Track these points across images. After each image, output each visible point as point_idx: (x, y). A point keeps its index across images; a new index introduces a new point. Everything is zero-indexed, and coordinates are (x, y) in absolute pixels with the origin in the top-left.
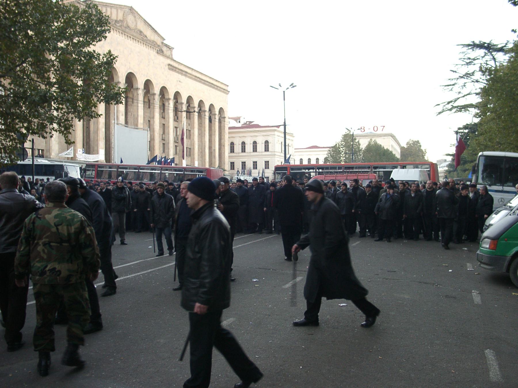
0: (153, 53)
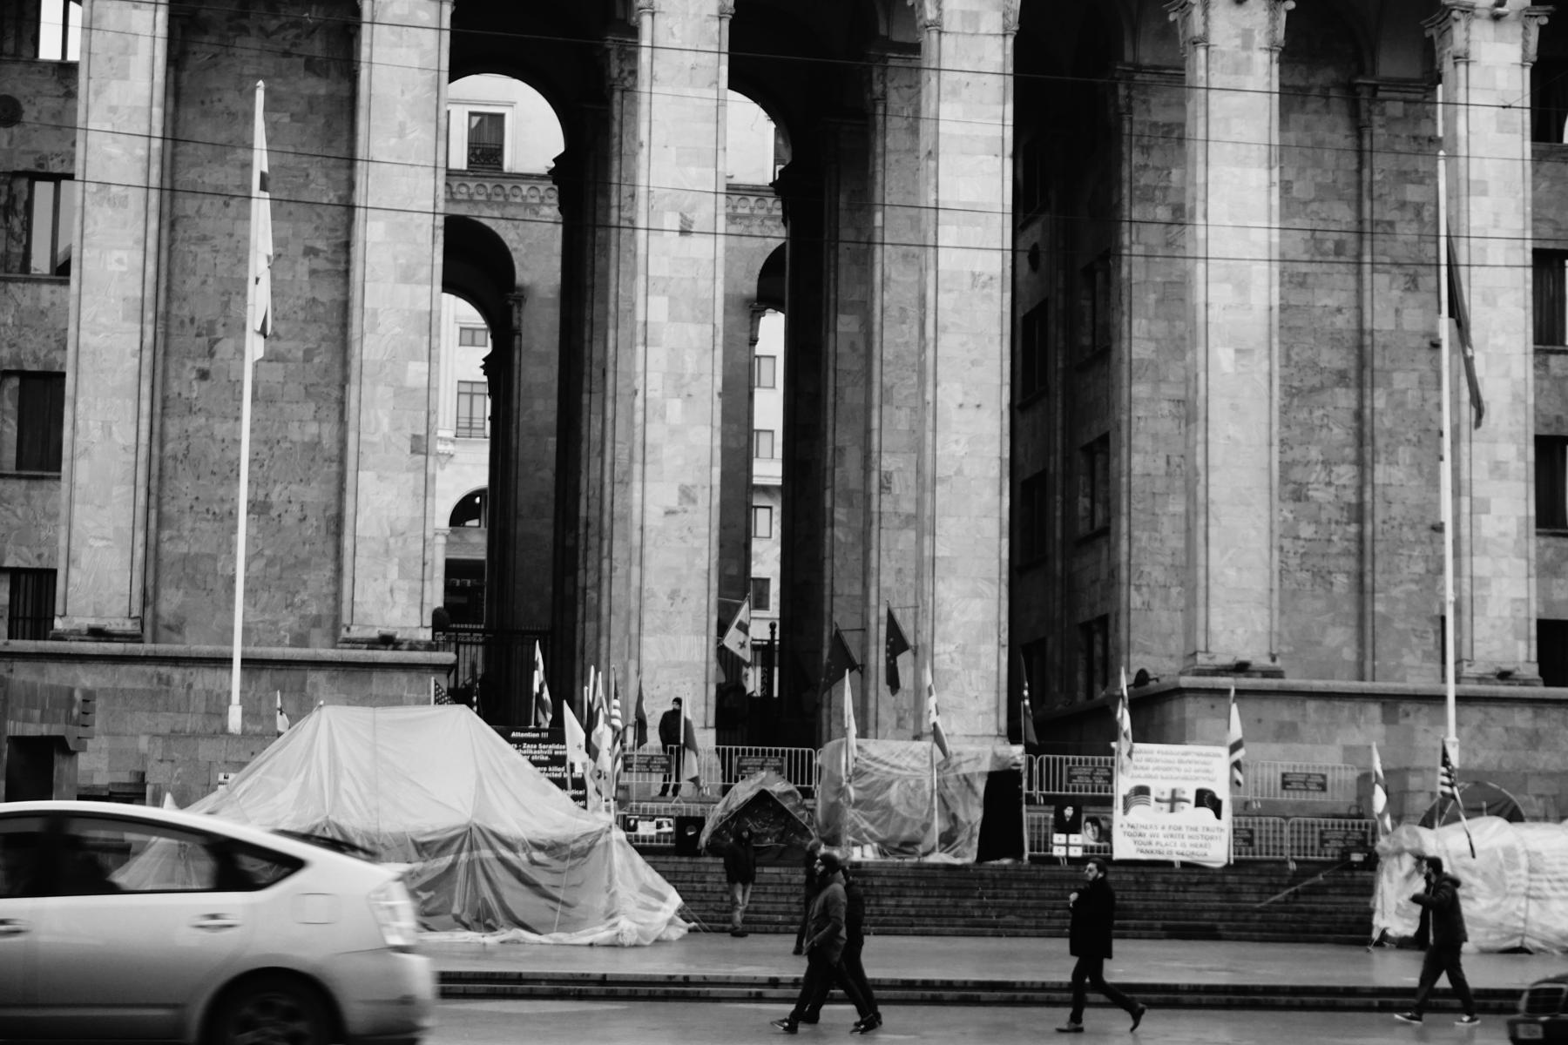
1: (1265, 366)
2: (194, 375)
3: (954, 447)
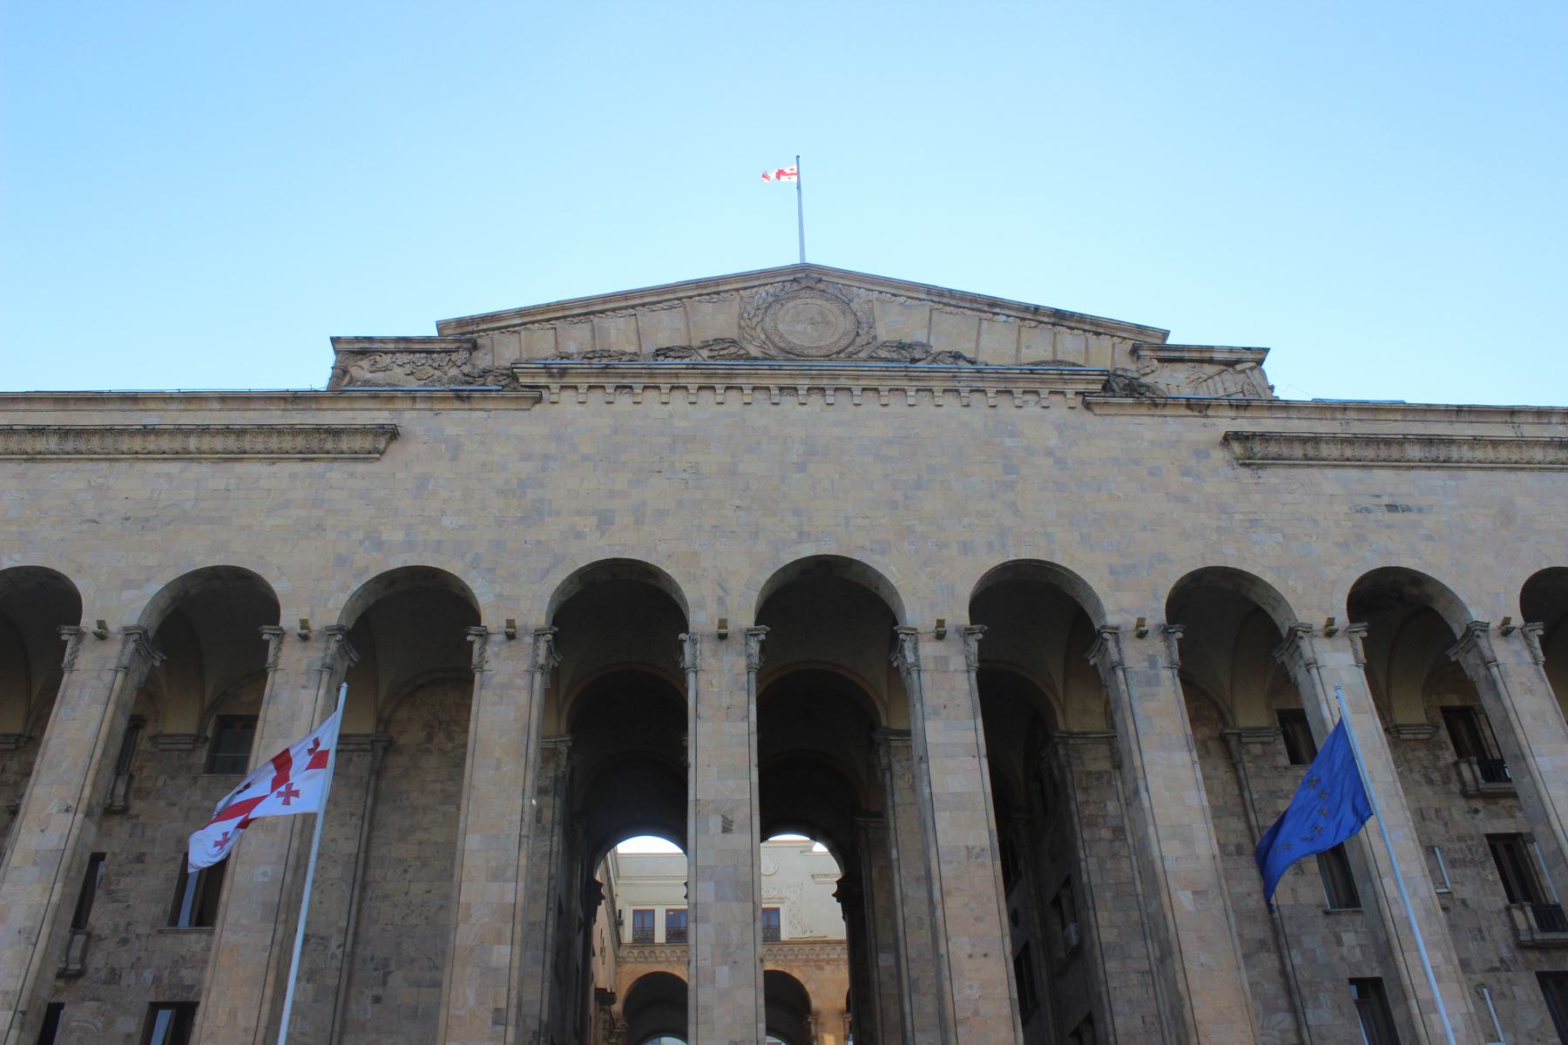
0: (1042, 423)
1: (1220, 902)
2: (369, 1001)
3: (968, 991)
